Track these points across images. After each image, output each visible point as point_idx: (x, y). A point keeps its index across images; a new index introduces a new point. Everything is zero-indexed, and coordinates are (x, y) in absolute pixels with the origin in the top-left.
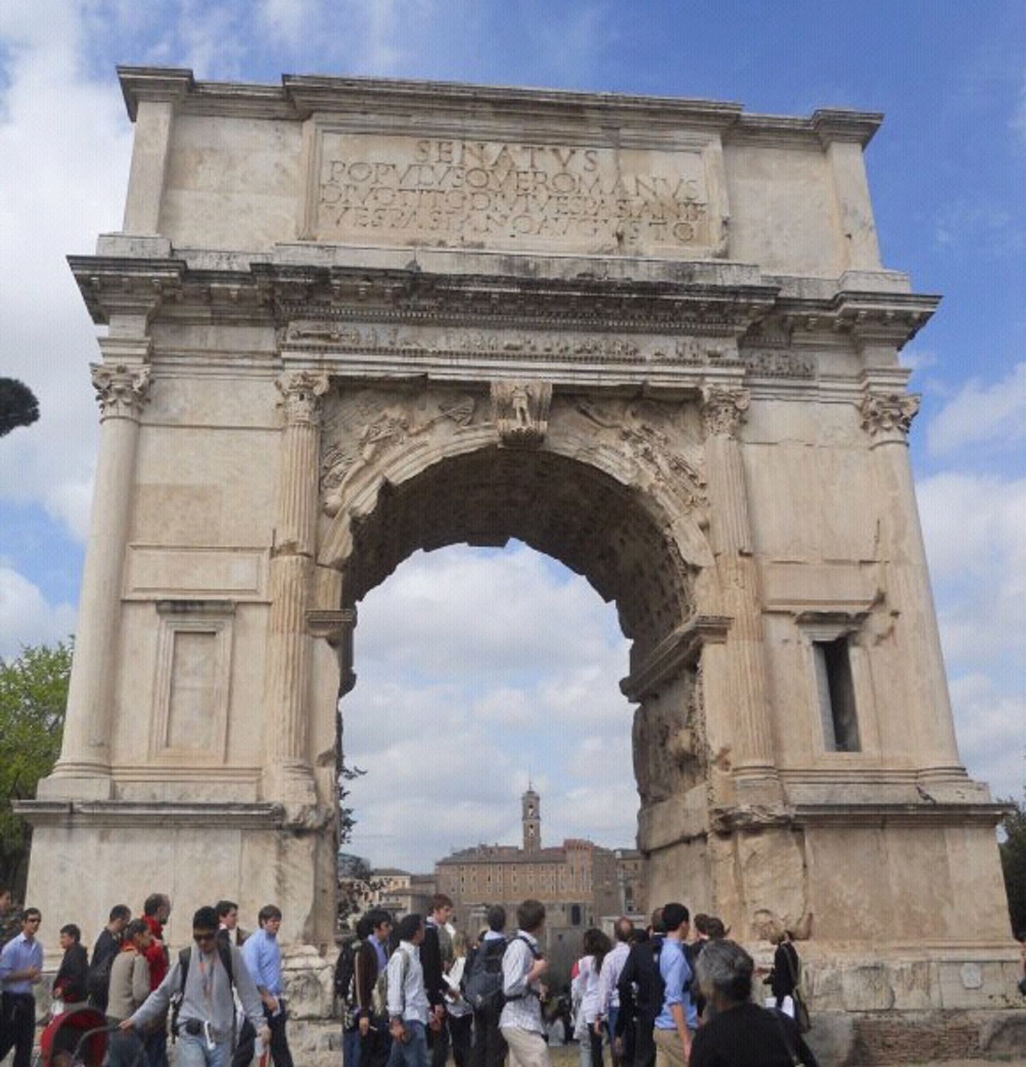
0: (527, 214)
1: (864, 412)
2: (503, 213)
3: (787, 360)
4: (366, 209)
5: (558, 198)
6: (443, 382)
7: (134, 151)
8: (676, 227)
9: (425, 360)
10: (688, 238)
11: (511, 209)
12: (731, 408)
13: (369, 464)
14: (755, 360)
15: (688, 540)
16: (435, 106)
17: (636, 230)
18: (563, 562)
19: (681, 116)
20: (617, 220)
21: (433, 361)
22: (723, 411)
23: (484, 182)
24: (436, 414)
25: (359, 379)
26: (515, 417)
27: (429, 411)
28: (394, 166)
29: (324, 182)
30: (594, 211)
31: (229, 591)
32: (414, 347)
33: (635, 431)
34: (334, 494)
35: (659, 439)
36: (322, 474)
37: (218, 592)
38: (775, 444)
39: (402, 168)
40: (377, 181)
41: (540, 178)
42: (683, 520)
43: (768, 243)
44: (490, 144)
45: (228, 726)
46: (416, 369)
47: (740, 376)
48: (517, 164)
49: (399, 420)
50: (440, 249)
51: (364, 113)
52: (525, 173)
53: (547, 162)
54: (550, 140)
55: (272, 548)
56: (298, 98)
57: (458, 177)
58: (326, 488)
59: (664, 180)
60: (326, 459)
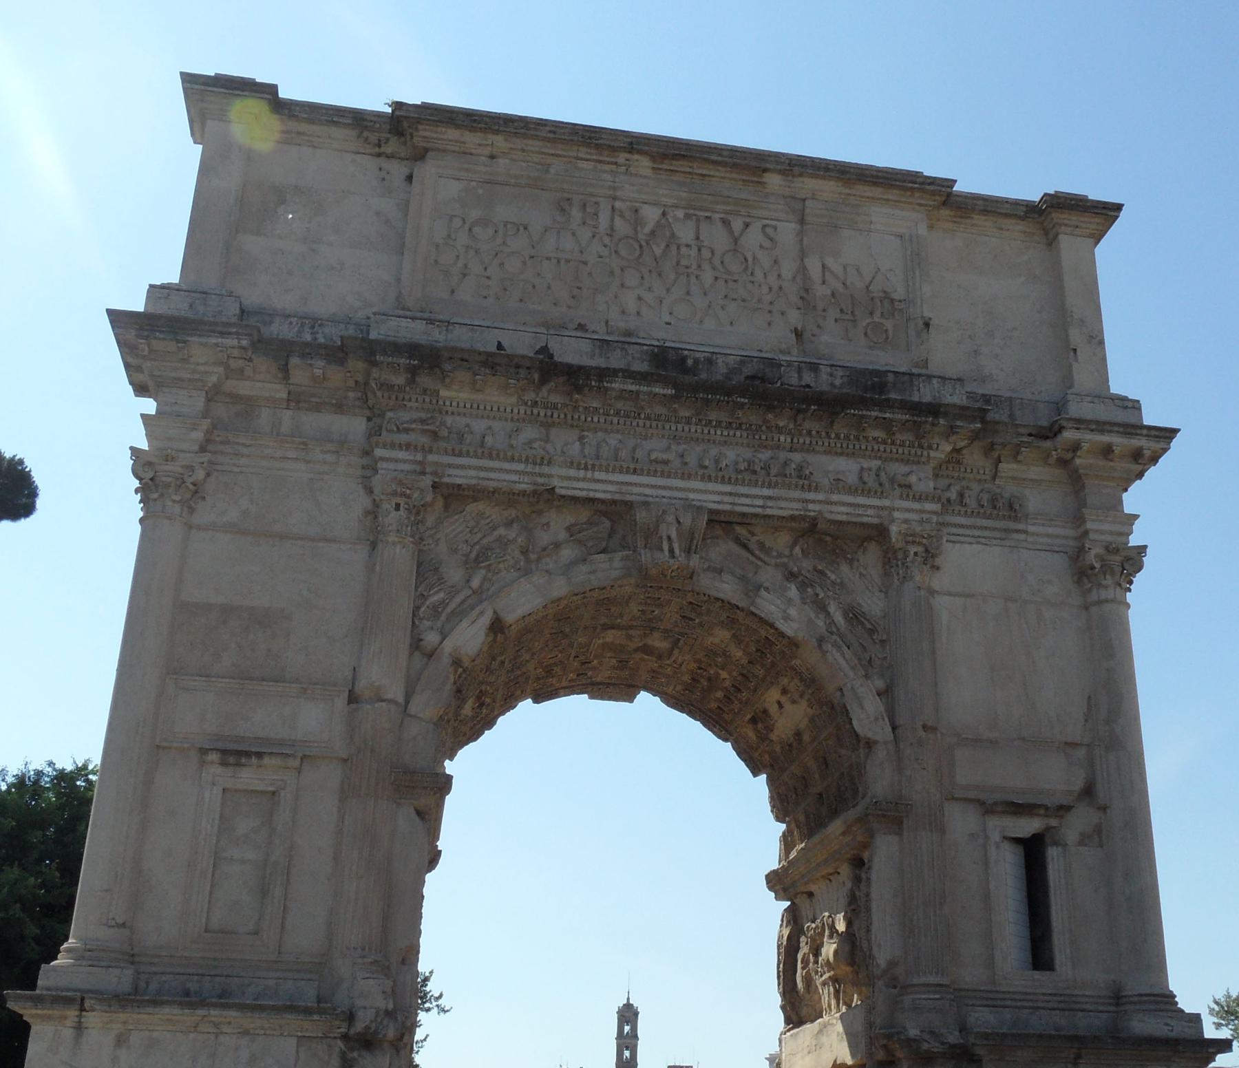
0: (687, 298)
4: (488, 278)
6: (574, 499)
11: (668, 290)
12: (920, 549)
14: (953, 494)
15: (862, 708)
16: (581, 155)
17: (819, 326)
18: (705, 725)
19: (880, 190)
22: (912, 553)
23: (637, 253)
24: (562, 536)
25: (469, 487)
26: (662, 550)
28: (526, 228)
30: (768, 298)
33: (804, 572)
35: (834, 583)
38: (973, 596)
40: (504, 243)
41: (706, 253)
44: (646, 206)
46: (541, 480)
47: (935, 513)
50: (579, 334)
52: (688, 246)
54: (720, 207)
57: (605, 246)
58: (421, 619)
60: (423, 585)
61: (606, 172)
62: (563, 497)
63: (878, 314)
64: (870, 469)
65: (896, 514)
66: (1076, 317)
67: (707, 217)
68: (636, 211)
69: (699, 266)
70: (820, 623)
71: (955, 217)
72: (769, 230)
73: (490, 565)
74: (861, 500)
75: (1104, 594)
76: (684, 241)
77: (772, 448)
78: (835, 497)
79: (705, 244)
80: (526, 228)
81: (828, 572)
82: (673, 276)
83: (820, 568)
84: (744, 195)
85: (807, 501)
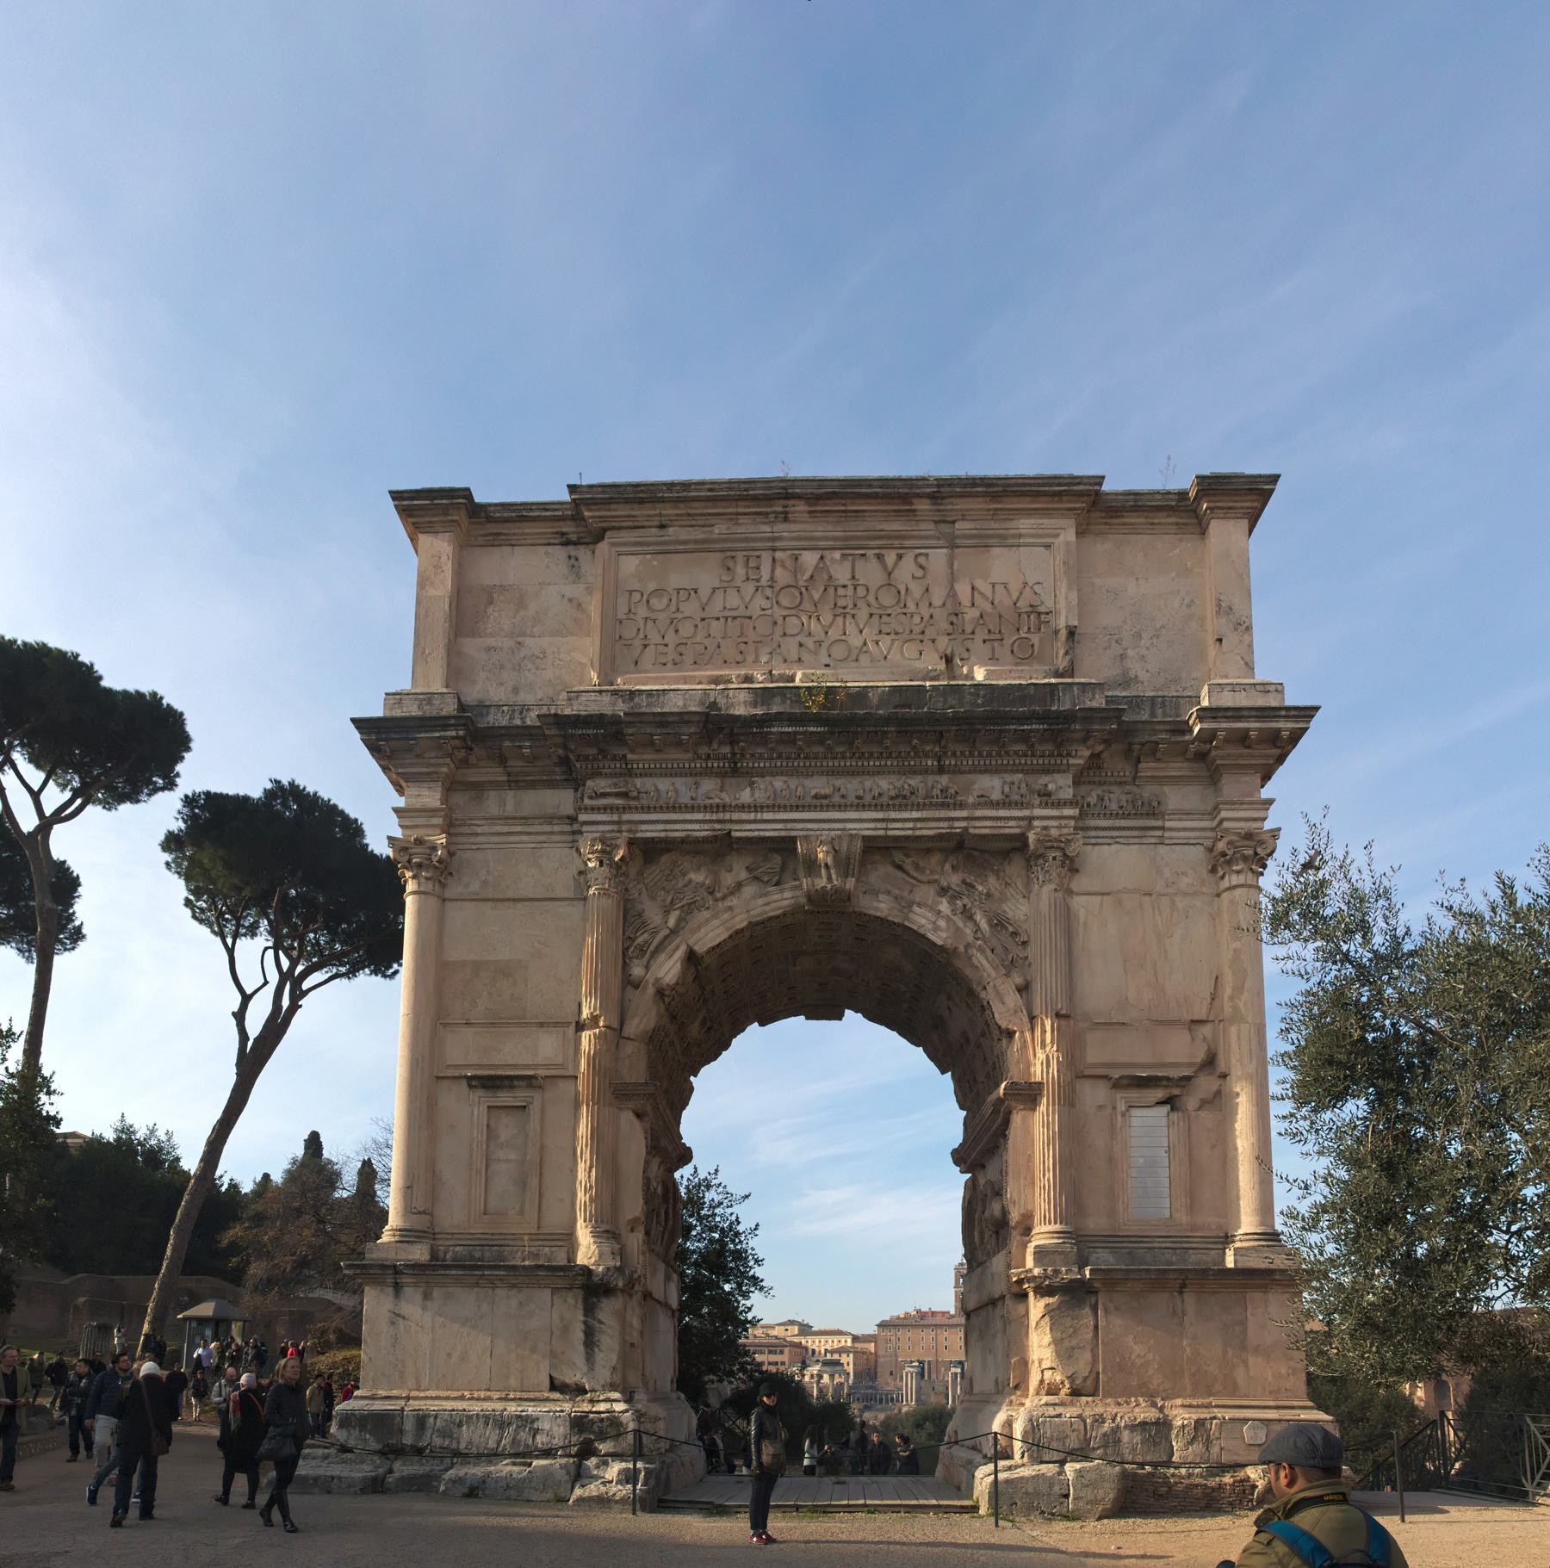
0: (843, 638)
1: (1215, 853)
2: (816, 639)
3: (1129, 797)
4: (666, 645)
6: (749, 840)
7: (418, 594)
8: (1015, 642)
9: (727, 816)
10: (1024, 654)
13: (674, 932)
14: (1093, 799)
15: (1003, 1003)
17: (968, 650)
20: (946, 639)
21: (736, 816)
23: (799, 599)
25: (661, 840)
26: (821, 877)
27: (736, 870)
28: (696, 592)
31: (536, 1066)
32: (718, 801)
34: (638, 965)
36: (626, 945)
37: (527, 1067)
39: (705, 593)
41: (861, 592)
42: (999, 982)
45: (541, 1195)
46: (717, 826)
49: (704, 883)
51: (662, 527)
52: (844, 586)
53: (870, 573)
55: (577, 1023)
56: (586, 514)
57: (768, 598)
58: (630, 958)
61: (765, 523)
62: (740, 839)
63: (1026, 629)
64: (1013, 784)
66: (1223, 605)
67: (863, 555)
68: (797, 559)
69: (855, 605)
71: (1105, 518)
72: (922, 560)
73: (682, 906)
74: (1002, 813)
75: (1235, 879)
76: (842, 582)
78: (978, 813)
80: (696, 592)
82: (830, 618)
84: (896, 526)
85: (953, 819)
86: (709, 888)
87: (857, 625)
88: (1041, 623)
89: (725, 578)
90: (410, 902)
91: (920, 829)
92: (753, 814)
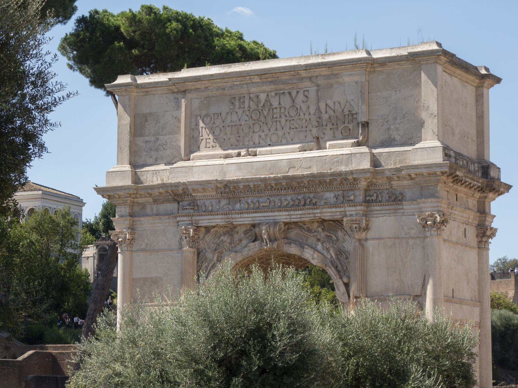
4: (210, 139)
5: (290, 121)
11: (269, 130)
15: (339, 290)
22: (354, 228)
23: (259, 116)
24: (243, 235)
28: (221, 114)
29: (193, 127)
41: (283, 110)
43: (389, 129)
48: (273, 103)
52: (276, 108)
54: (286, 88)
57: (248, 115)
59: (339, 103)
63: (347, 122)
65: (347, 213)
66: (425, 105)
67: (284, 93)
70: (329, 257)
76: (275, 106)
77: (303, 193)
78: (324, 210)
79: (282, 106)
81: (332, 235)
83: (329, 235)
85: (315, 213)
86: (229, 243)
87: (281, 126)
88: (353, 118)
89: (231, 107)
90: (120, 256)
91: (303, 218)
92: (240, 215)
